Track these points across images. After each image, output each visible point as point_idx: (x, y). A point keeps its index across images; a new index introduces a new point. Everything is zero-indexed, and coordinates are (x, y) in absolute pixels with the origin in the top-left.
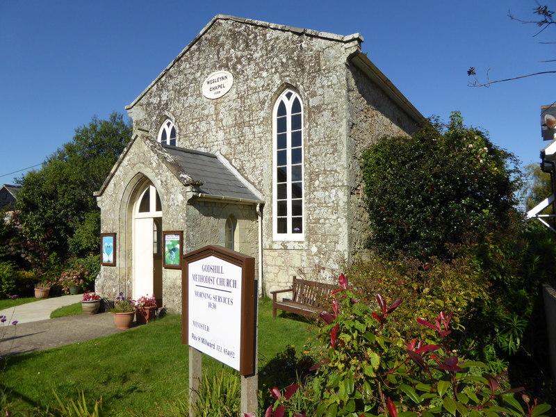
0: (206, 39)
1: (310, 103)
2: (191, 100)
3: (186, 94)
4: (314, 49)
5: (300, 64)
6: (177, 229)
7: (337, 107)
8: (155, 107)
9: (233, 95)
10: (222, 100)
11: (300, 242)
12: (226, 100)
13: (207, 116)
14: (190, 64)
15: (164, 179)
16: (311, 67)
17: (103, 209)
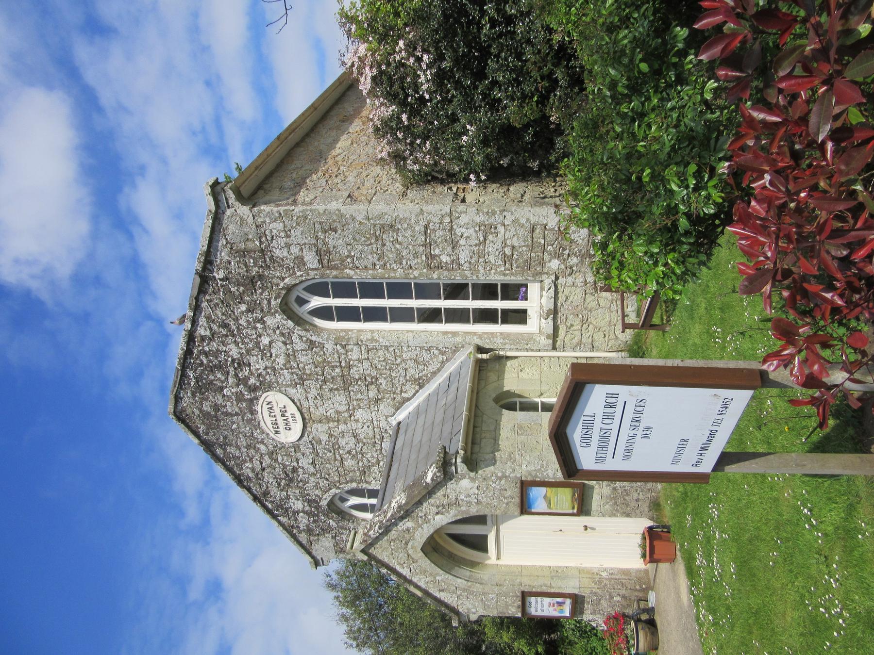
0: (207, 434)
1: (314, 266)
2: (305, 462)
3: (294, 470)
5: (251, 282)
7: (321, 223)
8: (314, 521)
9: (297, 393)
10: (304, 410)
11: (542, 289)
12: (305, 404)
13: (331, 435)
14: (245, 461)
15: (435, 510)
16: (255, 265)
17: (481, 612)
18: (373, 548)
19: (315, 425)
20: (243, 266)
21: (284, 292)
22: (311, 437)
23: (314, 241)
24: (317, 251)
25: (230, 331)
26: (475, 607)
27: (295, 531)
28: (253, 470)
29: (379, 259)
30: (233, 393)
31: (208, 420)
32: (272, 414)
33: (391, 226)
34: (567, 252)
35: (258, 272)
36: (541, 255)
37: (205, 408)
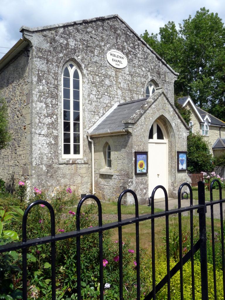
9: (127, 71)
10: (120, 70)
13: (110, 76)
28: (91, 32)
32: (118, 57)
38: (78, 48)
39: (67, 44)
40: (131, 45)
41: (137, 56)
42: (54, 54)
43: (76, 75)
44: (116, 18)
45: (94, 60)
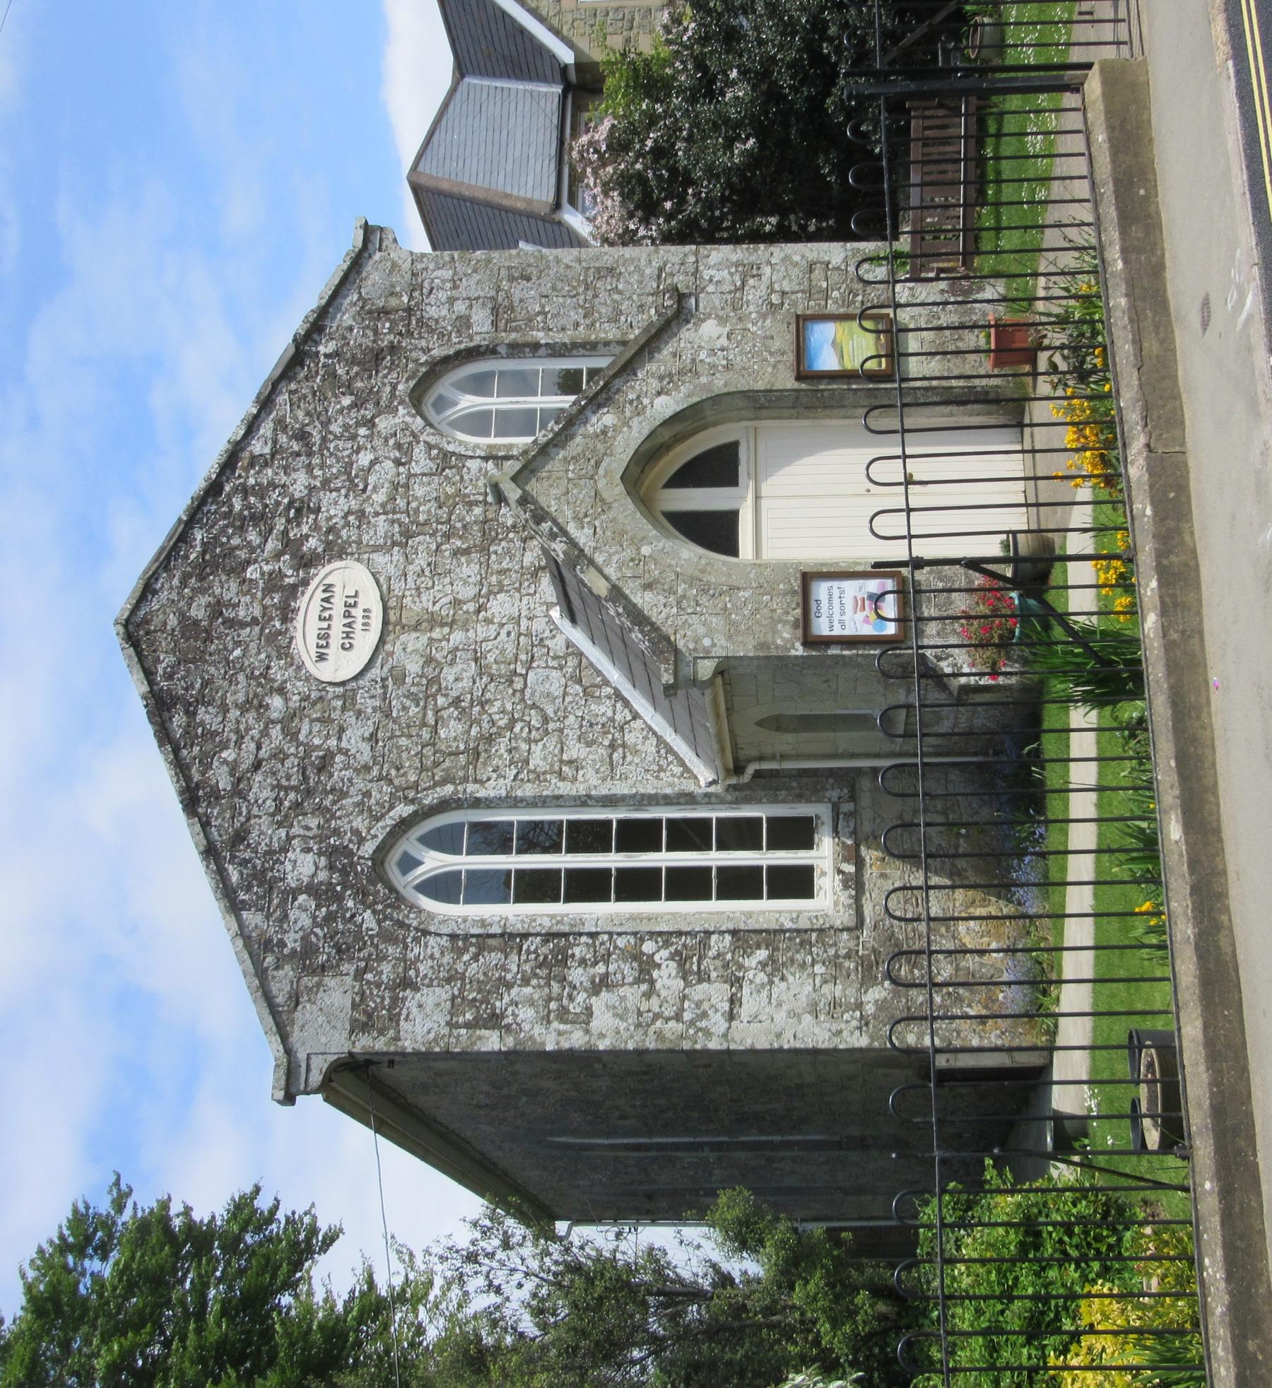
0: (170, 677)
3: (324, 765)
4: (350, 322)
5: (374, 359)
6: (790, 337)
7: (509, 268)
8: (330, 918)
9: (387, 562)
10: (392, 603)
12: (398, 587)
13: (429, 660)
14: (224, 746)
15: (654, 384)
18: (534, 480)
19: (403, 638)
20: (370, 333)
21: (424, 369)
22: (386, 669)
23: (492, 293)
24: (493, 309)
25: (307, 445)
26: (710, 633)
27: (270, 960)
28: (233, 767)
29: (585, 317)
30: (263, 574)
31: (187, 640)
32: (326, 614)
33: (611, 270)
34: (860, 298)
35: (392, 342)
36: (823, 303)
37: (193, 613)
38: (320, 836)
39: (311, 889)
40: (253, 536)
41: (301, 500)
42: (370, 955)
43: (445, 841)
44: (131, 628)
45: (366, 747)
